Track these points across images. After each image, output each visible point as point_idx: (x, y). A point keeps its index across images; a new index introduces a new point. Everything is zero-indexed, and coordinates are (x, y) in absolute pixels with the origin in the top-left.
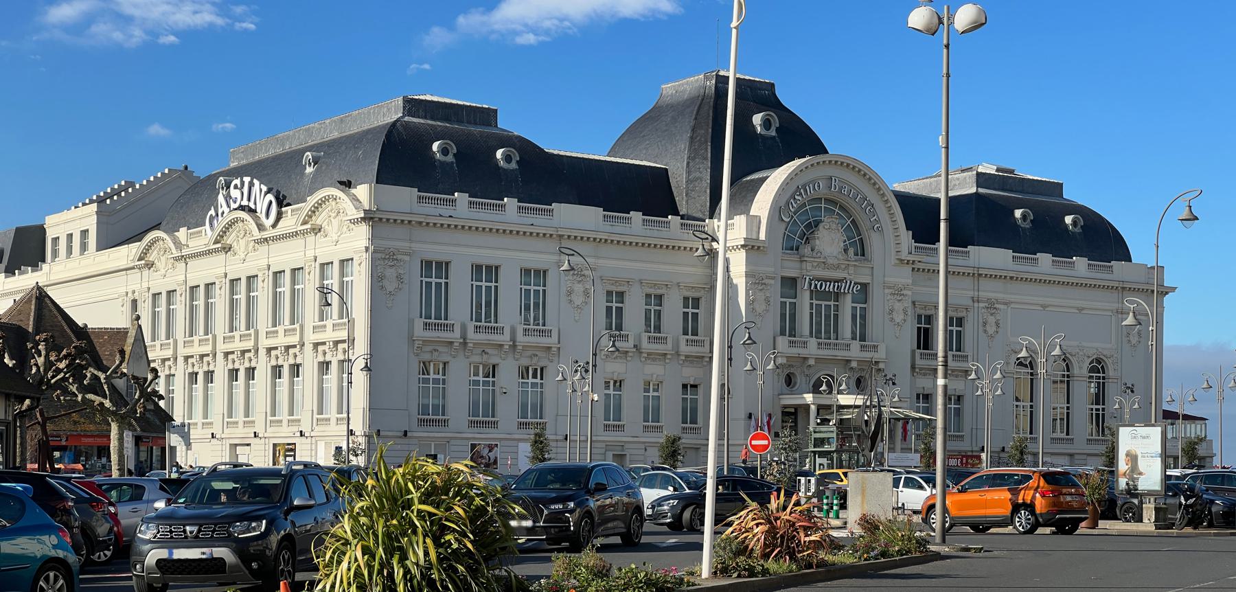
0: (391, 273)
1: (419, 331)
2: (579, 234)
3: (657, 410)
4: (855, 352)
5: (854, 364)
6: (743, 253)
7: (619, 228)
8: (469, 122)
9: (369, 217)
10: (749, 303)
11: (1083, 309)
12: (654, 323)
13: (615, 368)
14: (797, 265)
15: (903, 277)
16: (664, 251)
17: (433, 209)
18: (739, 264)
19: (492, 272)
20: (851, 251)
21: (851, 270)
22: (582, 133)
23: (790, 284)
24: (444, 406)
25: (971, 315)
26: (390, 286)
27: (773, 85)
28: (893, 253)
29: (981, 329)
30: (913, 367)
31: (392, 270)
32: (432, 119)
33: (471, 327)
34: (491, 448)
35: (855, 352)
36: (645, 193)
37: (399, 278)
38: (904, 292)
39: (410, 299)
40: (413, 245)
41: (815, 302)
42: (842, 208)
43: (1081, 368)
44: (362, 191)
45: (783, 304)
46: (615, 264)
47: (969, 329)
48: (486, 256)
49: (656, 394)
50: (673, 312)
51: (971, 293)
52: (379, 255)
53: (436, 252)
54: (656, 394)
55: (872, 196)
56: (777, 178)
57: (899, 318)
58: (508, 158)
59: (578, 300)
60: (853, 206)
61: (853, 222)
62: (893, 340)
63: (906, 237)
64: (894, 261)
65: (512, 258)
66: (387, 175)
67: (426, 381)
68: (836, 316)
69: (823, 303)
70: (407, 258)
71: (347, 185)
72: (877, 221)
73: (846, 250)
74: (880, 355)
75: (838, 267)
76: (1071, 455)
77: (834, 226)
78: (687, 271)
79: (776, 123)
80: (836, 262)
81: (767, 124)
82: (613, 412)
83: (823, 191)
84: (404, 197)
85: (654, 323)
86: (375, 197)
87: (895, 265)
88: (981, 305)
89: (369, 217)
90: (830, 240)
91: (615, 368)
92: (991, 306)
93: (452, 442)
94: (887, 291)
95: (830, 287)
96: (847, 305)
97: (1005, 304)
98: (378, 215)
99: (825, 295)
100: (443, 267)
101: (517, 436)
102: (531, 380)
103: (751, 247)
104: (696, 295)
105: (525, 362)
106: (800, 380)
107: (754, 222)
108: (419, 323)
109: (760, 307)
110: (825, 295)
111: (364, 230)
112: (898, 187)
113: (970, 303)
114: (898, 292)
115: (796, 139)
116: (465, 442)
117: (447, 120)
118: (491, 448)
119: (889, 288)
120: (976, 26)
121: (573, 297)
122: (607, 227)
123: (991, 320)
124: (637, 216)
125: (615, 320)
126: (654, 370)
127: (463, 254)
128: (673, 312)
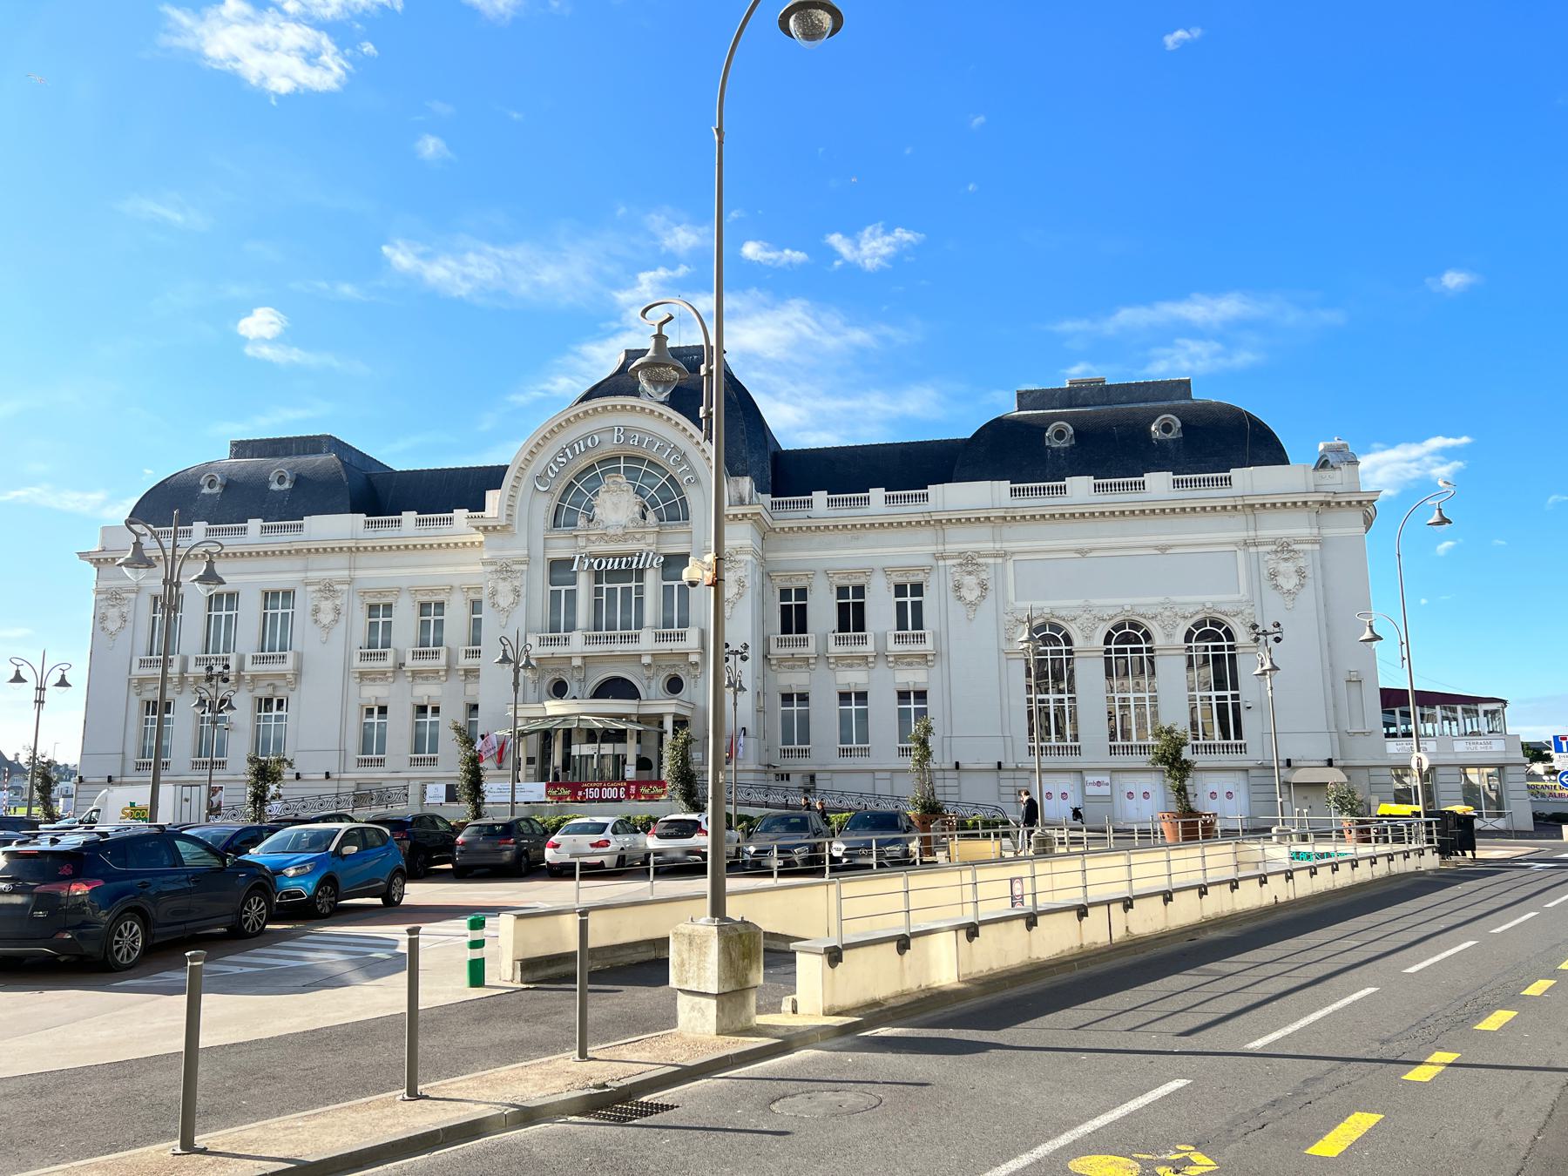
0: (113, 613)
11: (1171, 547)
14: (573, 541)
20: (651, 516)
23: (560, 569)
26: (112, 626)
29: (951, 595)
37: (123, 618)
41: (605, 586)
42: (652, 464)
43: (1169, 636)
45: (555, 595)
47: (929, 601)
51: (933, 549)
60: (653, 454)
61: (671, 479)
68: (640, 601)
69: (619, 586)
70: (133, 596)
72: (692, 470)
75: (625, 537)
80: (620, 531)
82: (371, 745)
88: (949, 562)
90: (616, 506)
92: (969, 562)
99: (613, 575)
102: (275, 712)
105: (264, 693)
106: (573, 688)
110: (613, 575)
113: (933, 562)
122: (370, 533)
123: (970, 581)
125: (378, 639)
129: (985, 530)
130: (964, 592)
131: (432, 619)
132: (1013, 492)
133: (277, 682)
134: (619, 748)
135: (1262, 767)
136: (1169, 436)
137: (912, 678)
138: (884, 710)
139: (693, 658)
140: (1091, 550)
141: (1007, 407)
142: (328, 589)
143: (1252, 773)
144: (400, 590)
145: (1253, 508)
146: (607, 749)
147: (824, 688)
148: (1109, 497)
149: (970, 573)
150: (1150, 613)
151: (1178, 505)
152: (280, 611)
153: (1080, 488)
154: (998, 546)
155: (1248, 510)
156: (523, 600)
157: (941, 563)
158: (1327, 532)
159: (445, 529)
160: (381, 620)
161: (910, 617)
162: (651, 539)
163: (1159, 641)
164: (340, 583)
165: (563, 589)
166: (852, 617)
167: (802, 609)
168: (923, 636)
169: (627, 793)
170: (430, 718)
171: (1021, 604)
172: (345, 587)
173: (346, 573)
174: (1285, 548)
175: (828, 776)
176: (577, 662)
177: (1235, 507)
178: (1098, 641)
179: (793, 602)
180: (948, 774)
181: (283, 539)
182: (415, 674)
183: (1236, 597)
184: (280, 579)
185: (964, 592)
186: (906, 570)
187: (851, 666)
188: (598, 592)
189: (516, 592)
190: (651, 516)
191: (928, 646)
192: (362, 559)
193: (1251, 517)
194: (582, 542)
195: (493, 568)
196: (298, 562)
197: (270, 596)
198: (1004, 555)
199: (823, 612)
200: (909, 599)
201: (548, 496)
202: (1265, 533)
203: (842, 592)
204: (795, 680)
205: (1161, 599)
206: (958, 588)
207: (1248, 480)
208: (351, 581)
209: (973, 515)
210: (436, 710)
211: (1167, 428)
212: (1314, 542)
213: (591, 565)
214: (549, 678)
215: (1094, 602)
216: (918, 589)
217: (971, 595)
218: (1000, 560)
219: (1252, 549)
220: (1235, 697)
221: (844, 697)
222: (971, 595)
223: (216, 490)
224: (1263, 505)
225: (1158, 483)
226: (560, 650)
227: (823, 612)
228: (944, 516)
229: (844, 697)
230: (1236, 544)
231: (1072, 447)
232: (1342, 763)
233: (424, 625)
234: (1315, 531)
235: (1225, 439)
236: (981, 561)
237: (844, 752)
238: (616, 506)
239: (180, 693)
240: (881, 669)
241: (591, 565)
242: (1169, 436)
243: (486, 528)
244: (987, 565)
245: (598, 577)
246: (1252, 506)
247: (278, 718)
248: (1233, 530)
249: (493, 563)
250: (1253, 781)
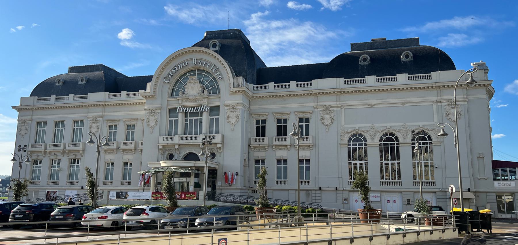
7: (115, 99)
11: (407, 103)
15: (238, 100)
23: (172, 111)
26: (23, 133)
29: (320, 122)
30: (249, 146)
34: (55, 192)
37: (26, 130)
41: (189, 118)
42: (207, 72)
43: (405, 138)
45: (171, 121)
46: (112, 114)
47: (311, 124)
51: (313, 104)
57: (233, 121)
60: (206, 68)
61: (214, 78)
67: (36, 167)
68: (201, 124)
69: (194, 118)
70: (30, 122)
72: (220, 74)
75: (196, 99)
76: (401, 192)
87: (230, 95)
88: (319, 109)
90: (193, 88)
92: (327, 109)
93: (40, 190)
94: (226, 108)
97: (338, 107)
98: (22, 107)
101: (63, 188)
105: (72, 157)
106: (176, 156)
110: (192, 114)
113: (313, 109)
114: (233, 108)
116: (45, 191)
118: (55, 192)
119: (227, 106)
122: (110, 99)
123: (327, 116)
129: (334, 97)
130: (325, 121)
131: (131, 131)
132: (345, 82)
133: (77, 153)
134: (188, 179)
135: (441, 191)
136: (408, 60)
137: (305, 154)
138: (293, 167)
139: (219, 146)
140: (375, 105)
141: (348, 50)
142: (95, 120)
143: (437, 193)
144: (120, 120)
145: (440, 87)
146: (183, 179)
147: (270, 158)
148: (382, 84)
149: (327, 114)
150: (398, 129)
151: (409, 87)
152: (79, 128)
153: (371, 80)
154: (338, 103)
155: (438, 88)
156: (158, 123)
157: (316, 110)
158: (471, 97)
159: (136, 97)
160: (113, 131)
161: (304, 130)
162: (205, 100)
163: (401, 140)
164: (99, 117)
165: (174, 119)
166: (282, 131)
167: (264, 128)
168: (308, 138)
169: (181, 196)
170: (129, 167)
171: (346, 126)
172: (101, 119)
173: (101, 114)
175: (271, 191)
176: (177, 147)
177: (432, 87)
178: (377, 141)
179: (261, 125)
180: (317, 192)
181: (81, 101)
182: (124, 151)
183: (432, 123)
184: (79, 116)
185: (325, 121)
186: (303, 113)
187: (281, 149)
188: (186, 120)
189: (156, 120)
190: (205, 91)
191: (310, 142)
192: (107, 109)
193: (439, 91)
194: (180, 102)
195: (148, 112)
197: (76, 122)
198: (341, 106)
199: (271, 128)
200: (304, 124)
201: (169, 85)
202: (444, 97)
203: (279, 121)
204: (260, 155)
205: (402, 124)
206: (322, 119)
207: (438, 76)
208: (103, 117)
209: (328, 91)
210: (131, 164)
211: (407, 56)
212: (464, 101)
213: (183, 110)
214: (167, 153)
216: (307, 120)
217: (327, 122)
218: (339, 109)
219: (439, 104)
221: (279, 161)
222: (327, 122)
223: (61, 84)
224: (444, 86)
225: (402, 78)
226: (170, 142)
227: (271, 128)
228: (317, 92)
229: (279, 161)
230: (432, 102)
231: (369, 64)
232: (474, 190)
233: (128, 133)
234: (465, 96)
235: (432, 60)
236: (332, 109)
237: (278, 183)
238: (193, 88)
239: (44, 157)
240: (292, 150)
241: (183, 110)
242: (408, 60)
243: (146, 96)
244: (334, 111)
245: (186, 114)
246: (439, 86)
247: (77, 167)
248: (432, 96)
249: (148, 110)
250: (438, 197)
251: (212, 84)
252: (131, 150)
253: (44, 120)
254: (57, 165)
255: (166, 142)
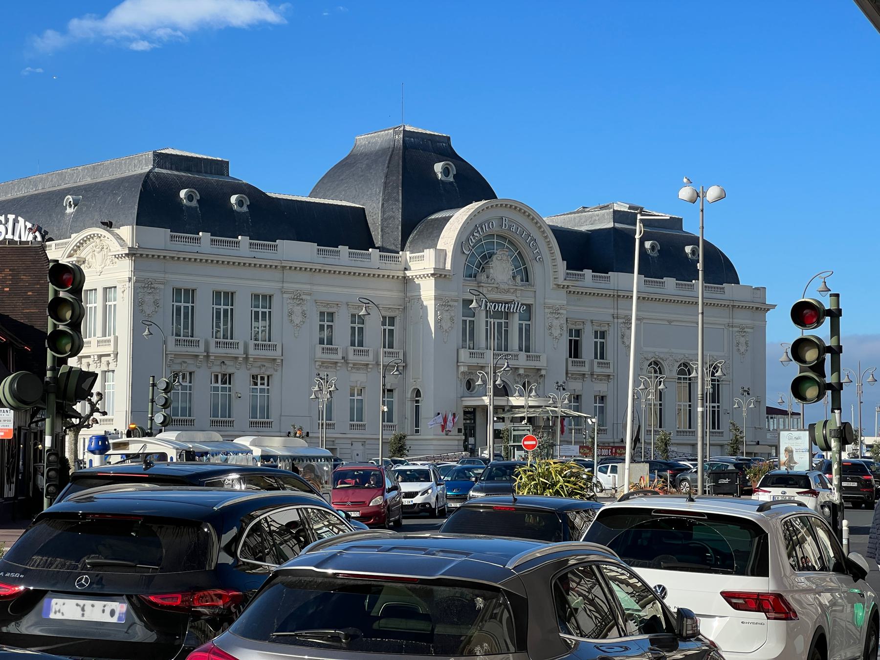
0: (149, 299)
1: (171, 346)
2: (298, 265)
3: (360, 411)
4: (522, 361)
5: (521, 371)
6: (432, 280)
7: (330, 260)
8: (206, 173)
9: (132, 254)
10: (437, 322)
12: (358, 338)
13: (576, 386)
15: (559, 299)
16: (356, 278)
17: (182, 245)
18: (428, 291)
19: (229, 297)
20: (518, 278)
21: (519, 293)
22: (291, 181)
24: (190, 409)
25: (611, 329)
26: (148, 309)
27: (449, 138)
28: (552, 279)
30: (567, 373)
31: (151, 297)
32: (177, 170)
33: (213, 342)
35: (522, 361)
36: (341, 229)
37: (156, 303)
38: (561, 311)
39: (165, 318)
40: (167, 276)
42: (510, 242)
44: (126, 232)
48: (225, 285)
49: (359, 398)
50: (374, 330)
51: (612, 311)
52: (139, 284)
53: (184, 281)
54: (359, 398)
55: (535, 234)
56: (458, 219)
57: (556, 333)
58: (240, 203)
59: (297, 320)
62: (552, 351)
63: (562, 265)
64: (552, 286)
65: (245, 286)
66: (144, 219)
68: (506, 331)
69: (497, 321)
70: (162, 286)
71: (108, 225)
72: (539, 253)
73: (514, 277)
74: (542, 364)
75: (507, 291)
77: (505, 258)
78: (386, 295)
79: (453, 171)
80: (506, 287)
81: (446, 171)
83: (496, 229)
84: (159, 236)
85: (358, 338)
86: (137, 237)
87: (553, 289)
88: (620, 321)
89: (132, 254)
90: (501, 269)
91: (576, 386)
94: (547, 310)
95: (501, 308)
96: (515, 322)
99: (497, 314)
100: (189, 294)
102: (259, 386)
103: (439, 275)
104: (392, 314)
107: (441, 255)
108: (171, 340)
109: (446, 325)
111: (127, 265)
112: (550, 220)
113: (611, 319)
114: (556, 311)
115: (470, 186)
117: (188, 170)
120: (720, 198)
121: (294, 317)
124: (344, 250)
126: (359, 378)
127: (206, 283)
128: (374, 330)
137: (601, 388)
139: (543, 372)
142: (298, 298)
157: (616, 320)
164: (305, 294)
174: (742, 330)
184: (264, 287)
196: (277, 274)
215: (673, 350)
220: (718, 407)
251: (517, 264)
252: (367, 365)
253: (194, 288)
254: (219, 385)
255: (474, 361)
